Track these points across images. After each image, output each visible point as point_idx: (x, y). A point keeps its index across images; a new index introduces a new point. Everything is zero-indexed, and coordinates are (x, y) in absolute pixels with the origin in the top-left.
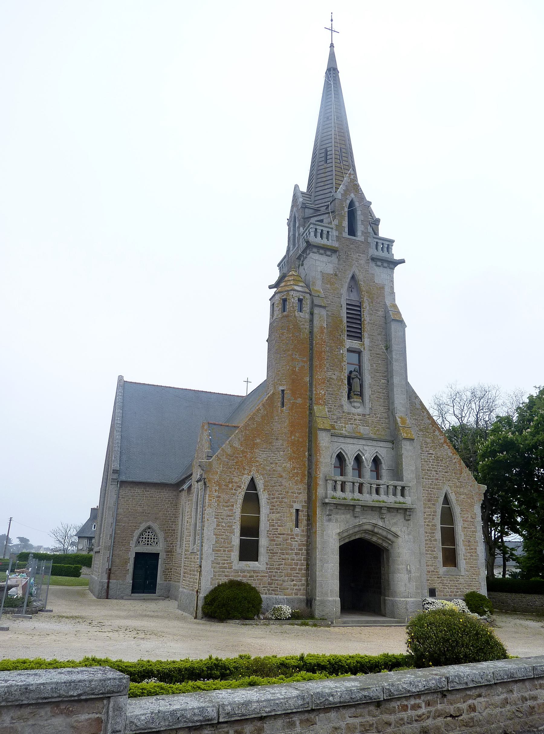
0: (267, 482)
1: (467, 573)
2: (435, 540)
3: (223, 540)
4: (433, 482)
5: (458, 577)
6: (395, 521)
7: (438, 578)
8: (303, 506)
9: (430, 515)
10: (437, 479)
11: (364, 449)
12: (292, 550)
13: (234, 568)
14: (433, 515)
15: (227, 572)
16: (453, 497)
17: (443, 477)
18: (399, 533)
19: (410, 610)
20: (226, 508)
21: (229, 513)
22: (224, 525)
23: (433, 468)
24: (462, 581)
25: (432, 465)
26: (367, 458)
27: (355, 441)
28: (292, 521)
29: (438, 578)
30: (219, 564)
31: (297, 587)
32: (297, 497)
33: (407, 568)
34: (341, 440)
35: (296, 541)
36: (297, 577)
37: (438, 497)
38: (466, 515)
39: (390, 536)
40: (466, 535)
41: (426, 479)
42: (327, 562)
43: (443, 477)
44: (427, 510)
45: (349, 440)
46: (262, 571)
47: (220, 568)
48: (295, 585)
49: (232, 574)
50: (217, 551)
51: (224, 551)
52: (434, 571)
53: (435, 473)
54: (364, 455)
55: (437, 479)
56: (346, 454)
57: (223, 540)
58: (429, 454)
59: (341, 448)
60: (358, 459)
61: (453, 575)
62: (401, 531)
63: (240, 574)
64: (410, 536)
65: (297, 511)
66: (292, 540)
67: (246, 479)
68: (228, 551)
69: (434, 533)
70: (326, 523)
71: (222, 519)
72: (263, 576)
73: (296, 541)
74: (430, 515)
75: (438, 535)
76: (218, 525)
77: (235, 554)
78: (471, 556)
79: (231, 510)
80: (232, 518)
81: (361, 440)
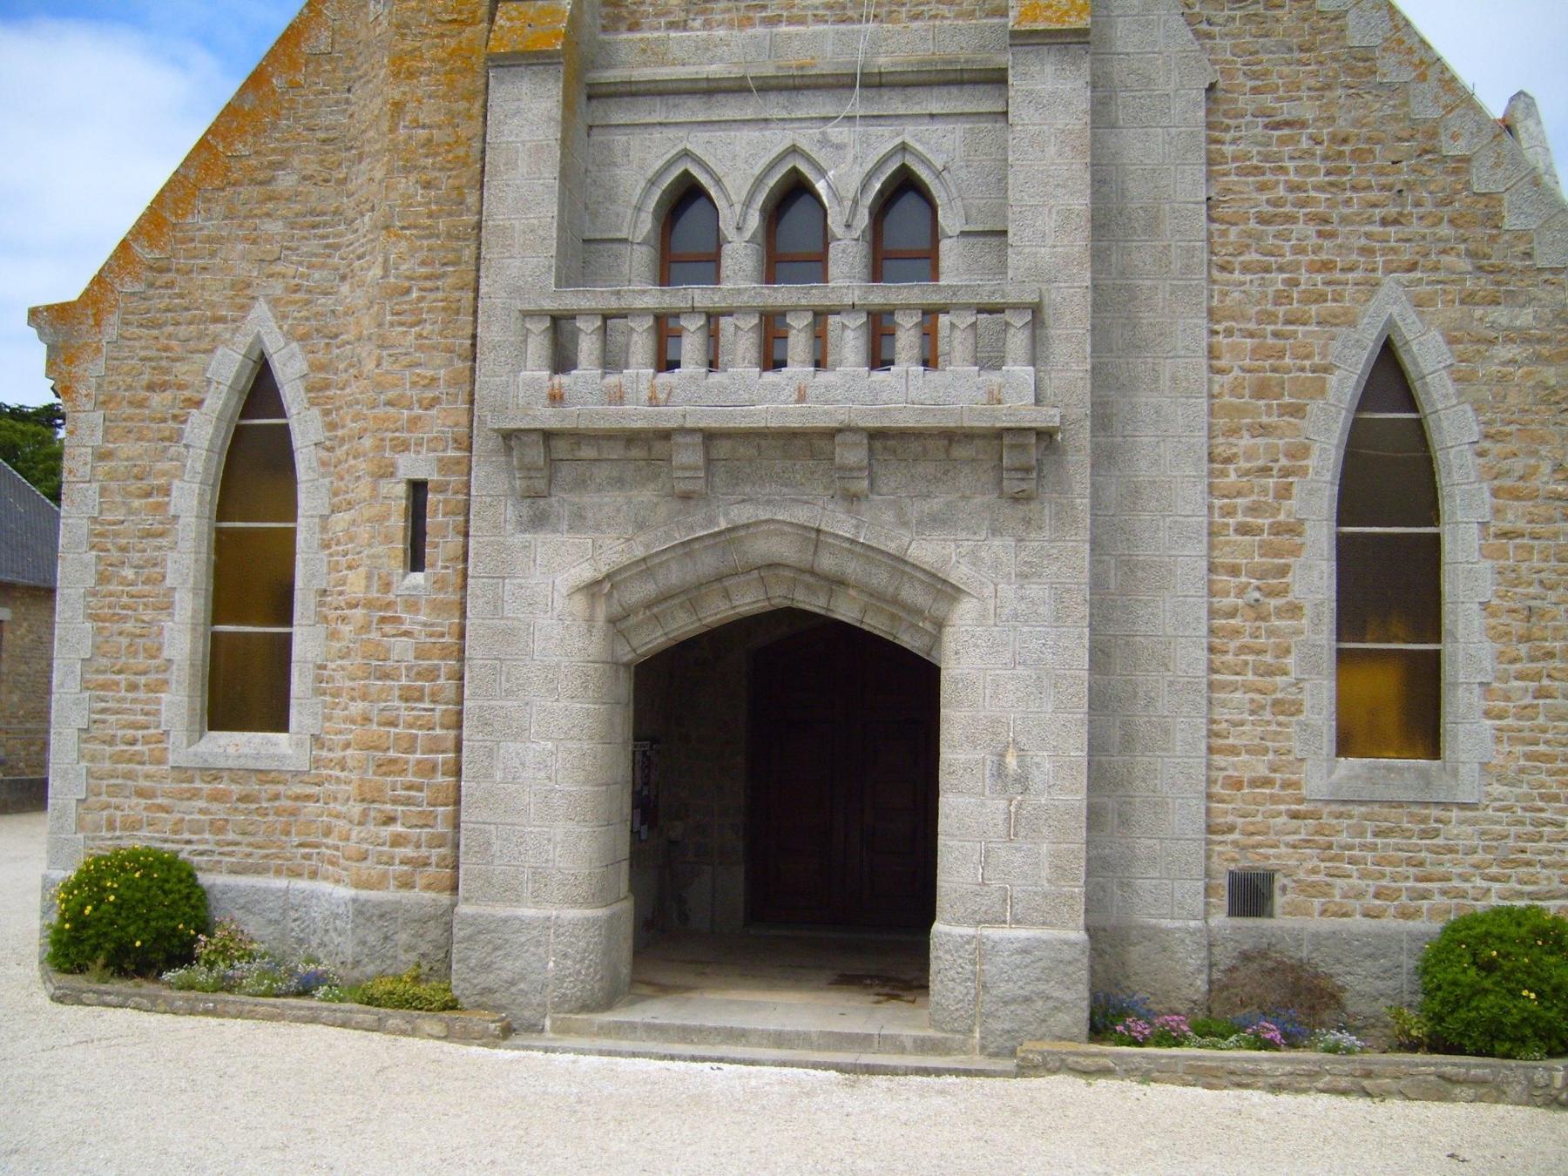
0: (322, 368)
1: (1497, 789)
2: (1294, 610)
3: (125, 641)
4: (1294, 283)
5: (1435, 812)
6: (936, 504)
7: (1295, 816)
8: (444, 466)
9: (1265, 471)
10: (1326, 266)
11: (824, 142)
12: (387, 676)
13: (172, 759)
14: (1285, 472)
15: (147, 776)
16: (1428, 358)
17: (1364, 251)
18: (959, 573)
19: (1003, 988)
20: (136, 503)
21: (150, 521)
22: (129, 573)
23: (1302, 204)
24: (1458, 830)
25: (1292, 188)
26: (845, 179)
27: (774, 107)
28: (388, 539)
29: (1295, 816)
30: (111, 741)
31: (409, 851)
32: (414, 422)
33: (1001, 765)
34: (693, 110)
35: (407, 634)
36: (408, 802)
37: (1326, 370)
38: (1518, 465)
39: (913, 594)
40: (1509, 579)
41: (1246, 269)
42: (519, 734)
43: (1364, 251)
44: (1246, 441)
45: (730, 109)
46: (296, 774)
47: (117, 758)
48: (397, 841)
49: (168, 785)
50: (103, 687)
51: (133, 687)
52: (1267, 782)
53: (1311, 230)
54: (822, 173)
55: (1326, 266)
57: (125, 641)
58: (1277, 126)
59: (686, 154)
60: (792, 194)
61: (1400, 804)
62: (976, 561)
63: (198, 784)
64: (1034, 590)
65: (418, 489)
66: (388, 628)
67: (225, 369)
68: (149, 688)
69: (1283, 571)
70: (520, 538)
71: (123, 549)
72: (297, 798)
73: (407, 634)
74: (1265, 471)
75: (1315, 579)
76: (103, 579)
77: (178, 700)
78: (1541, 694)
79: (160, 507)
80: (164, 542)
81: (802, 98)
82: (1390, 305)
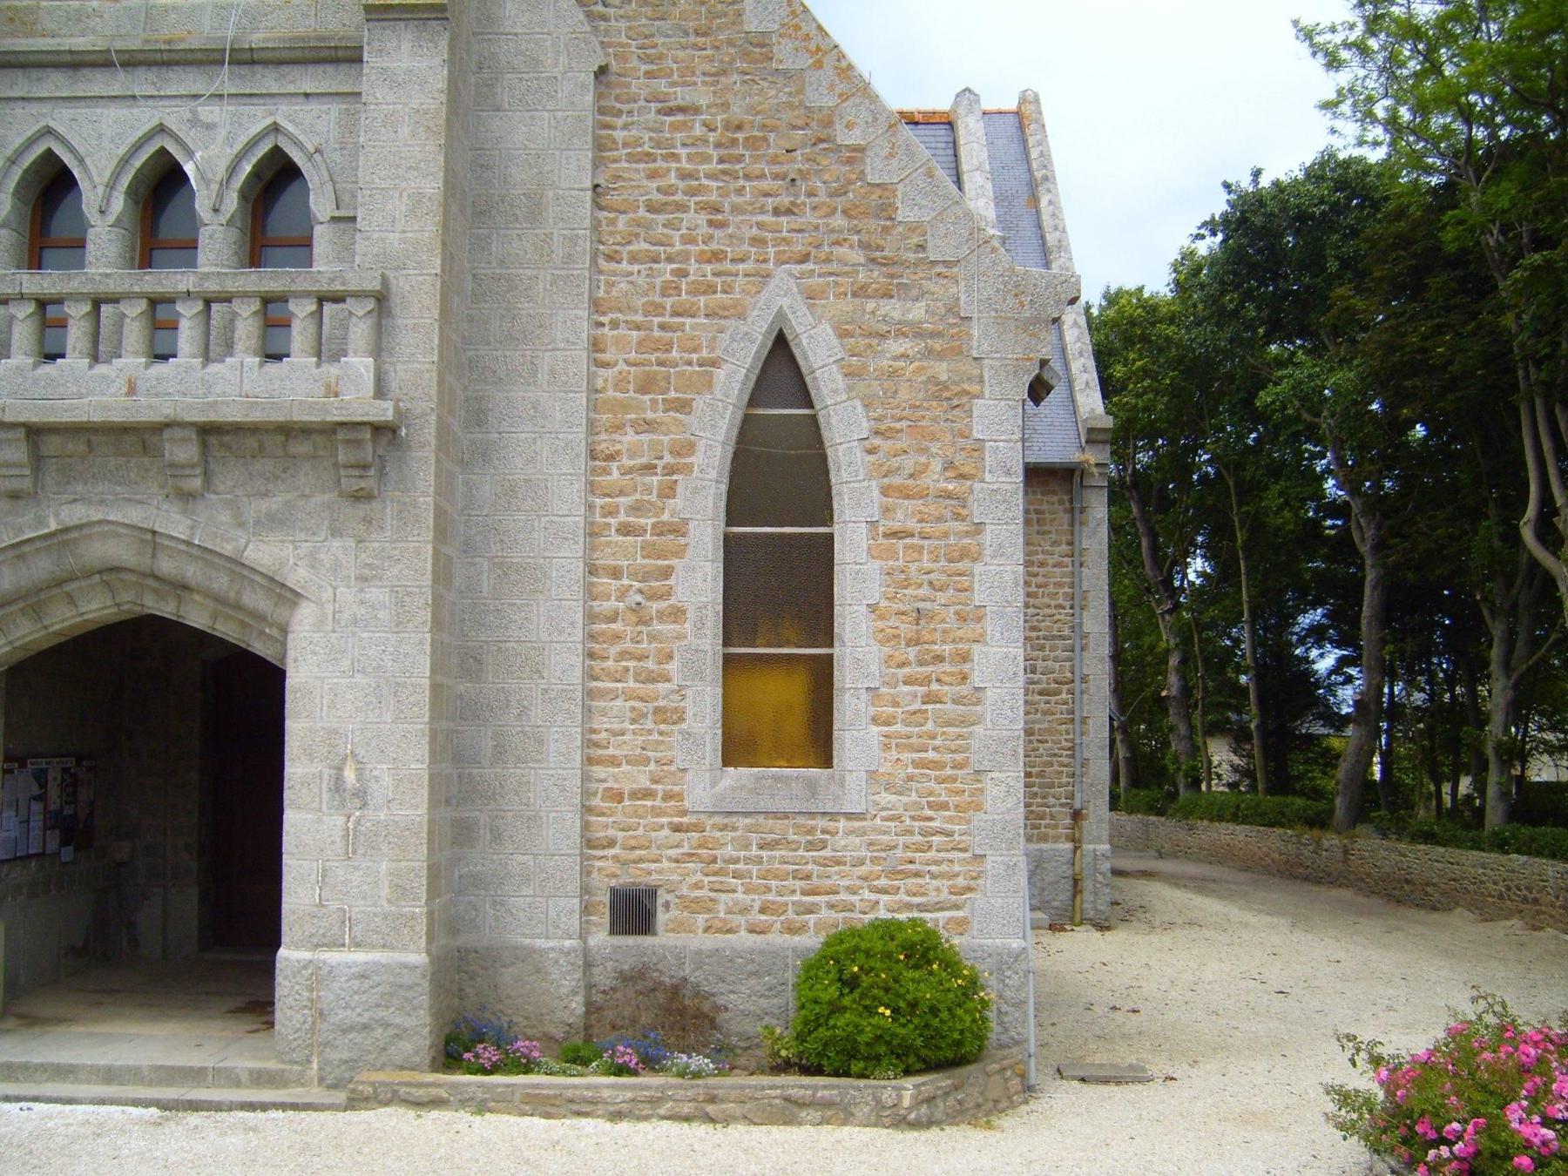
1: (886, 798)
2: (677, 614)
4: (683, 274)
5: (821, 823)
6: (274, 503)
7: (677, 829)
9: (649, 468)
10: (717, 257)
11: (195, 121)
14: (671, 470)
16: (819, 351)
17: (755, 241)
18: (297, 576)
19: (341, 1016)
24: (846, 842)
25: (684, 175)
26: (214, 164)
27: (142, 82)
29: (677, 829)
33: (338, 780)
34: (56, 83)
37: (714, 363)
39: (256, 600)
40: (899, 580)
41: (634, 259)
43: (755, 241)
44: (630, 437)
45: (97, 83)
52: (648, 794)
53: (702, 219)
55: (717, 257)
56: (125, 161)
58: (670, 112)
59: (49, 131)
61: (786, 816)
62: (314, 564)
64: (376, 593)
69: (667, 573)
74: (649, 468)
75: (700, 581)
78: (930, 699)
81: (174, 74)
82: (780, 297)
